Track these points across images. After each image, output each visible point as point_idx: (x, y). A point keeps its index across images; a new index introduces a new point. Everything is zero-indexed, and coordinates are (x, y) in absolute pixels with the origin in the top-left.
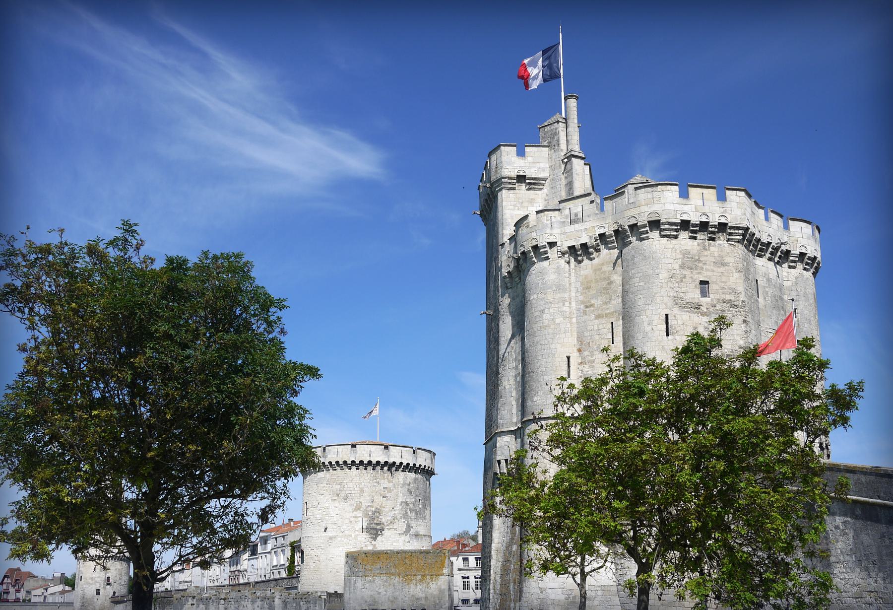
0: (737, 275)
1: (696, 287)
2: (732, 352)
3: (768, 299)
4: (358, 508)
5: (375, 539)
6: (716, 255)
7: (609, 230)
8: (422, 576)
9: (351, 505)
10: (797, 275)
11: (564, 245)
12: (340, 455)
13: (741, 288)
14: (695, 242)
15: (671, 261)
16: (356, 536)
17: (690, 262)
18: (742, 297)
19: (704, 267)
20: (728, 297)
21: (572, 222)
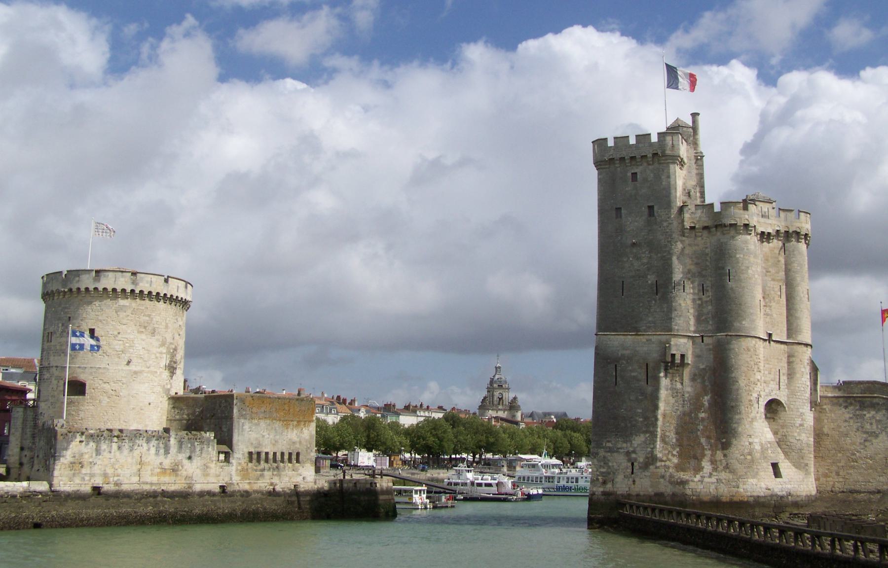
4: (163, 344)
5: (172, 377)
7: (783, 230)
8: (298, 422)
9: (158, 340)
11: (760, 229)
12: (154, 286)
16: (161, 373)
21: (762, 216)
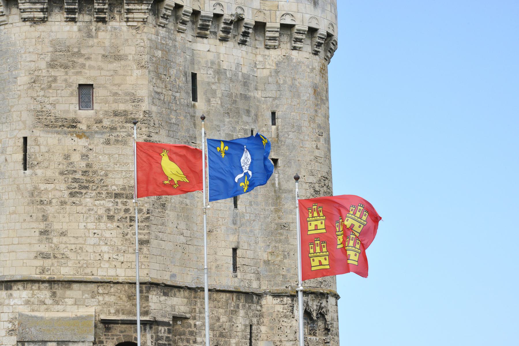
0: (137, 72)
1: (72, 94)
2: (124, 189)
3: (216, 102)
6: (107, 44)
10: (280, 58)
13: (143, 92)
14: (75, 27)
15: (34, 57)
17: (64, 57)
18: (145, 106)
19: (87, 63)
20: (122, 107)
